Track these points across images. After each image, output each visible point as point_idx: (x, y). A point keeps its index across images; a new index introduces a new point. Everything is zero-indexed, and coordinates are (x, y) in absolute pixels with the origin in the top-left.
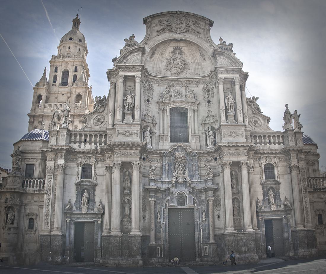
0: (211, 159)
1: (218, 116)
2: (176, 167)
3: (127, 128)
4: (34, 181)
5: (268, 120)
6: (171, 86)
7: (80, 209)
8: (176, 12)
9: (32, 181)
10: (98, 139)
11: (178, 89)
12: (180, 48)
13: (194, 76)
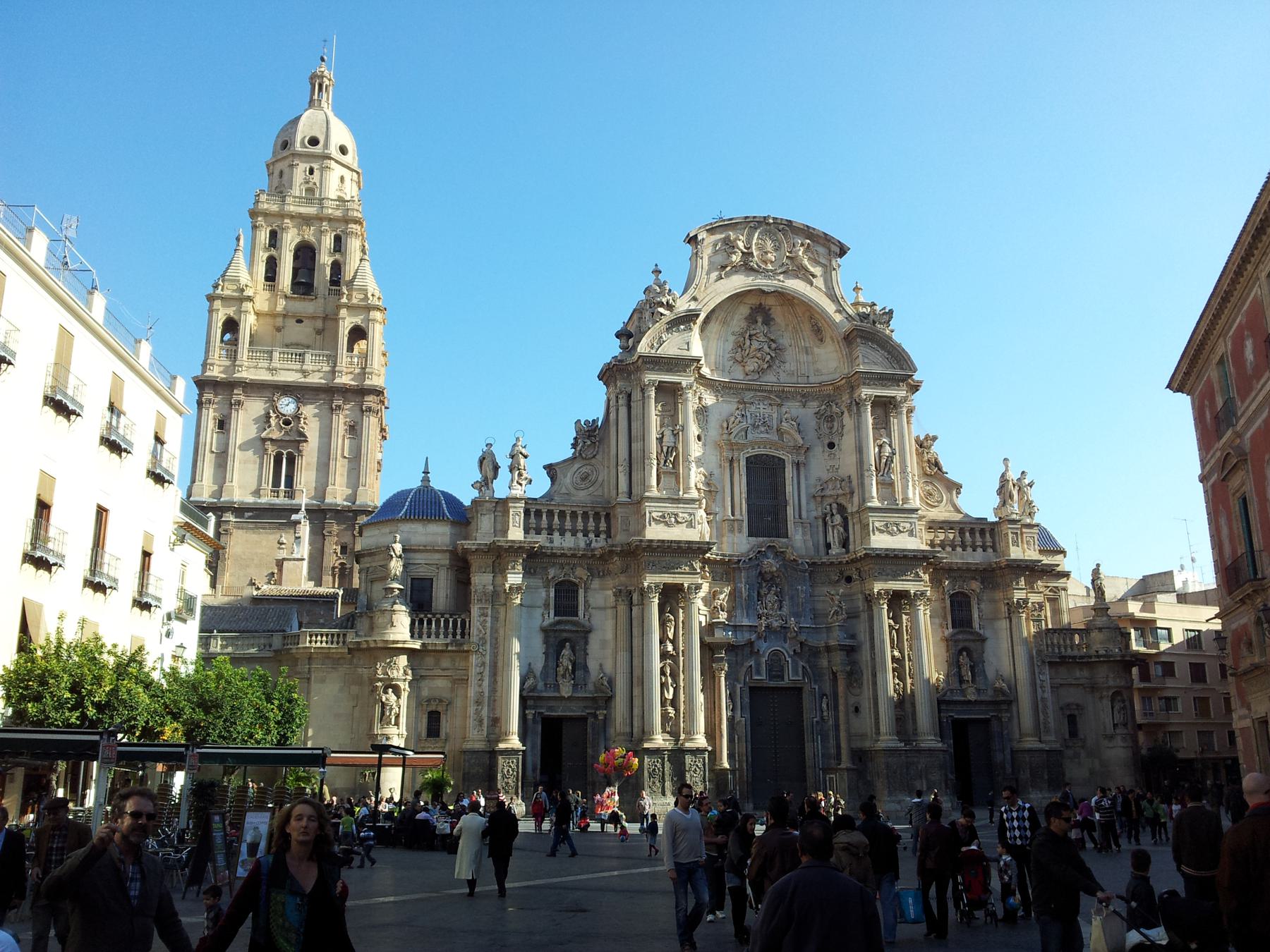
0: (837, 578)
1: (855, 483)
2: (762, 592)
3: (670, 508)
4: (438, 622)
5: (958, 487)
6: (745, 403)
7: (557, 687)
8: (765, 217)
9: (434, 620)
10: (591, 524)
11: (762, 411)
12: (767, 308)
13: (794, 380)
